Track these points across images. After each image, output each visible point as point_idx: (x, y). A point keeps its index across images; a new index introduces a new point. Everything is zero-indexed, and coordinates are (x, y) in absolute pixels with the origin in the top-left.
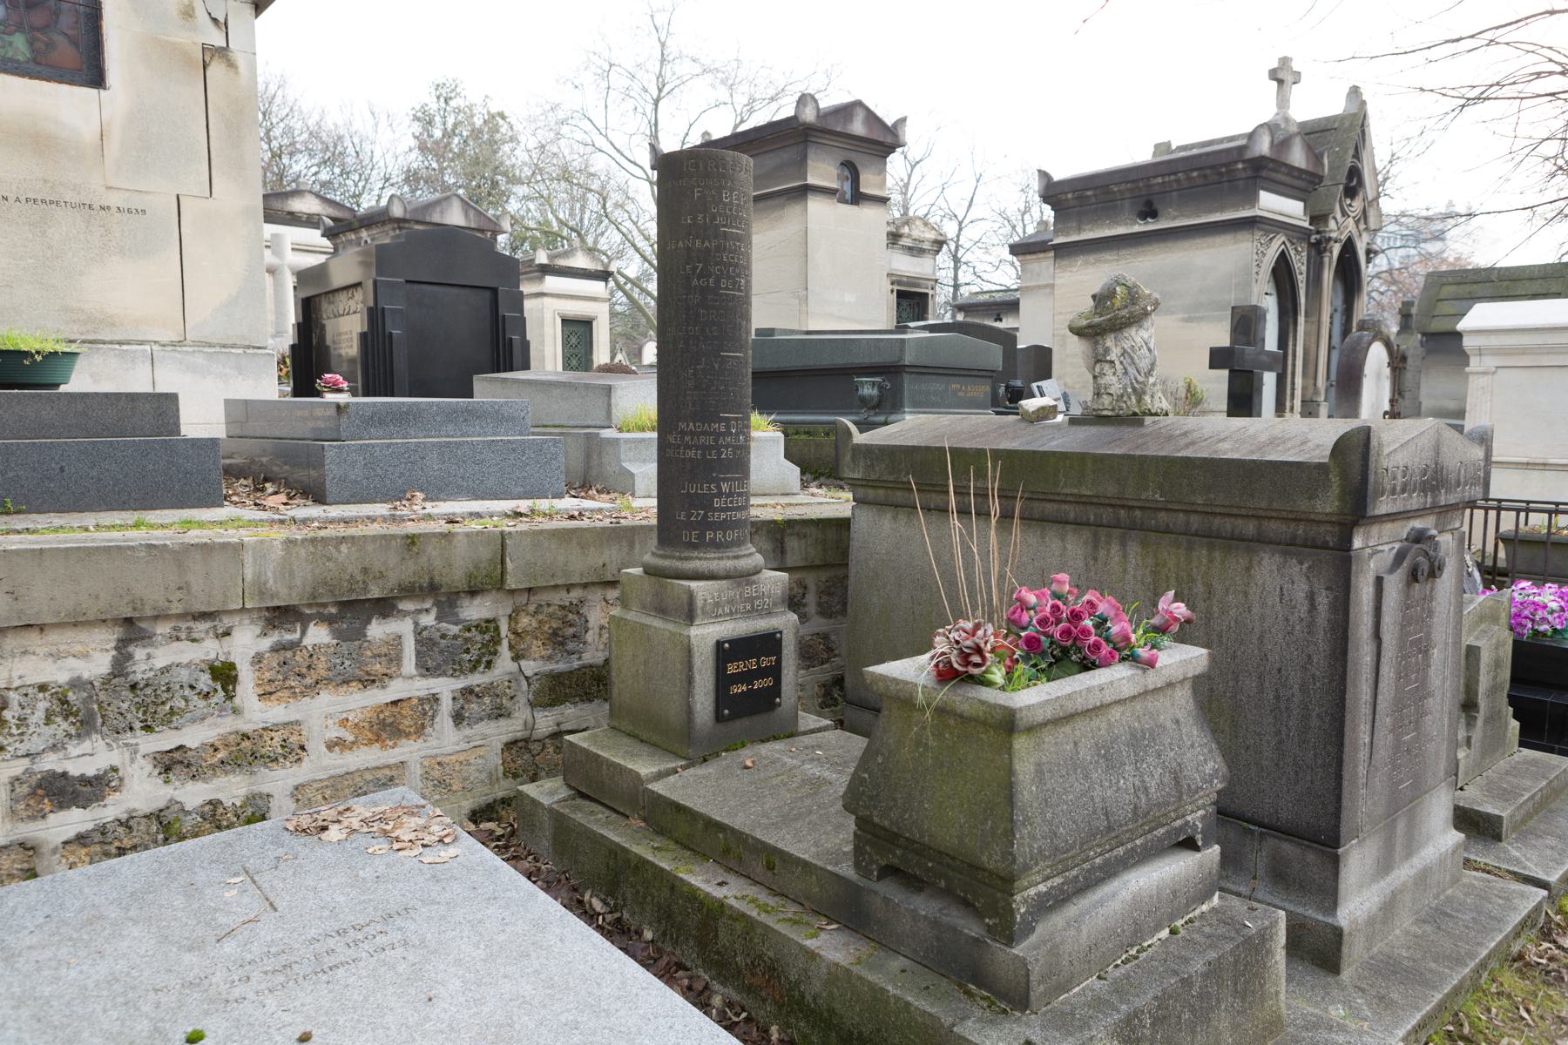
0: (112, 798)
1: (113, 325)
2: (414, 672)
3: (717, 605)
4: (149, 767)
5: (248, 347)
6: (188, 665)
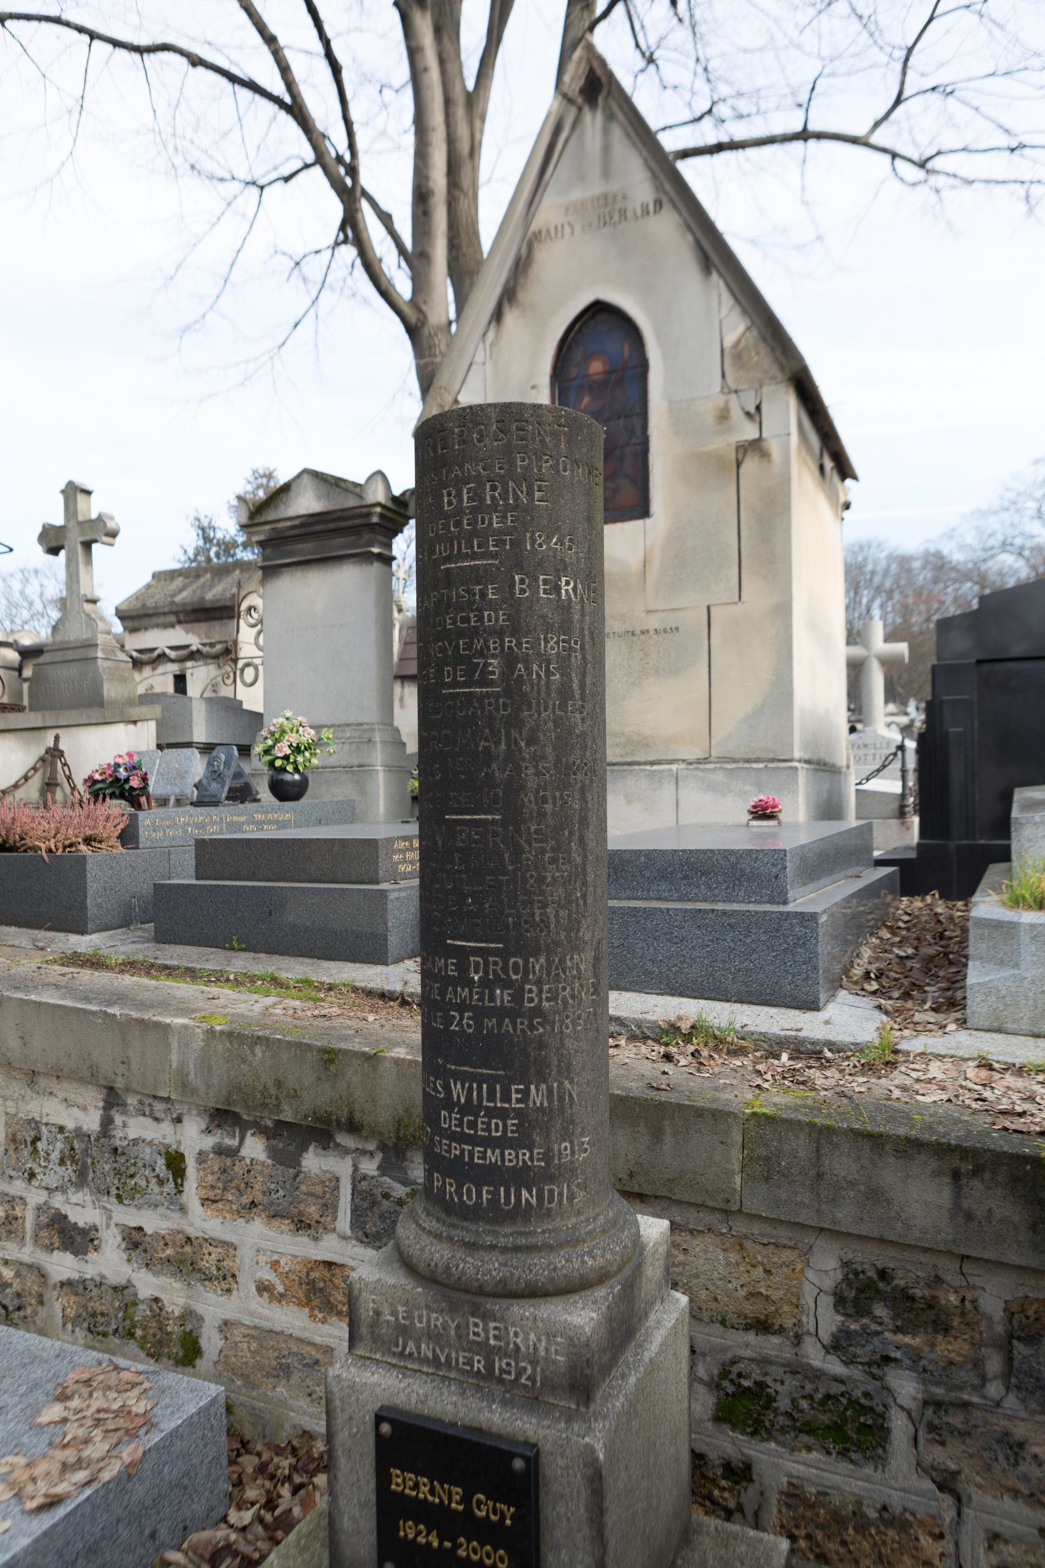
0: (92, 1256)
1: (647, 746)
2: (349, 1232)
3: (404, 1331)
4: (119, 1238)
5: (773, 760)
6: (151, 1143)
